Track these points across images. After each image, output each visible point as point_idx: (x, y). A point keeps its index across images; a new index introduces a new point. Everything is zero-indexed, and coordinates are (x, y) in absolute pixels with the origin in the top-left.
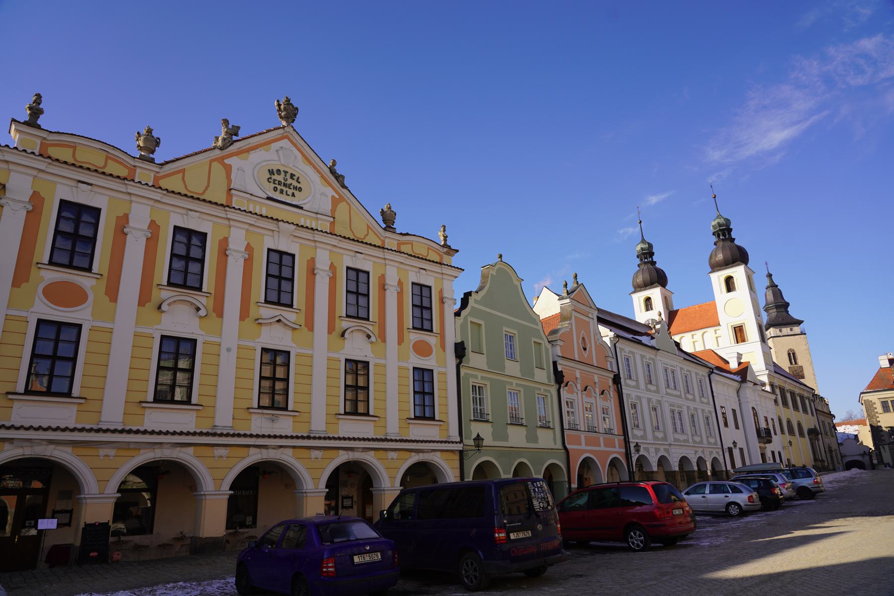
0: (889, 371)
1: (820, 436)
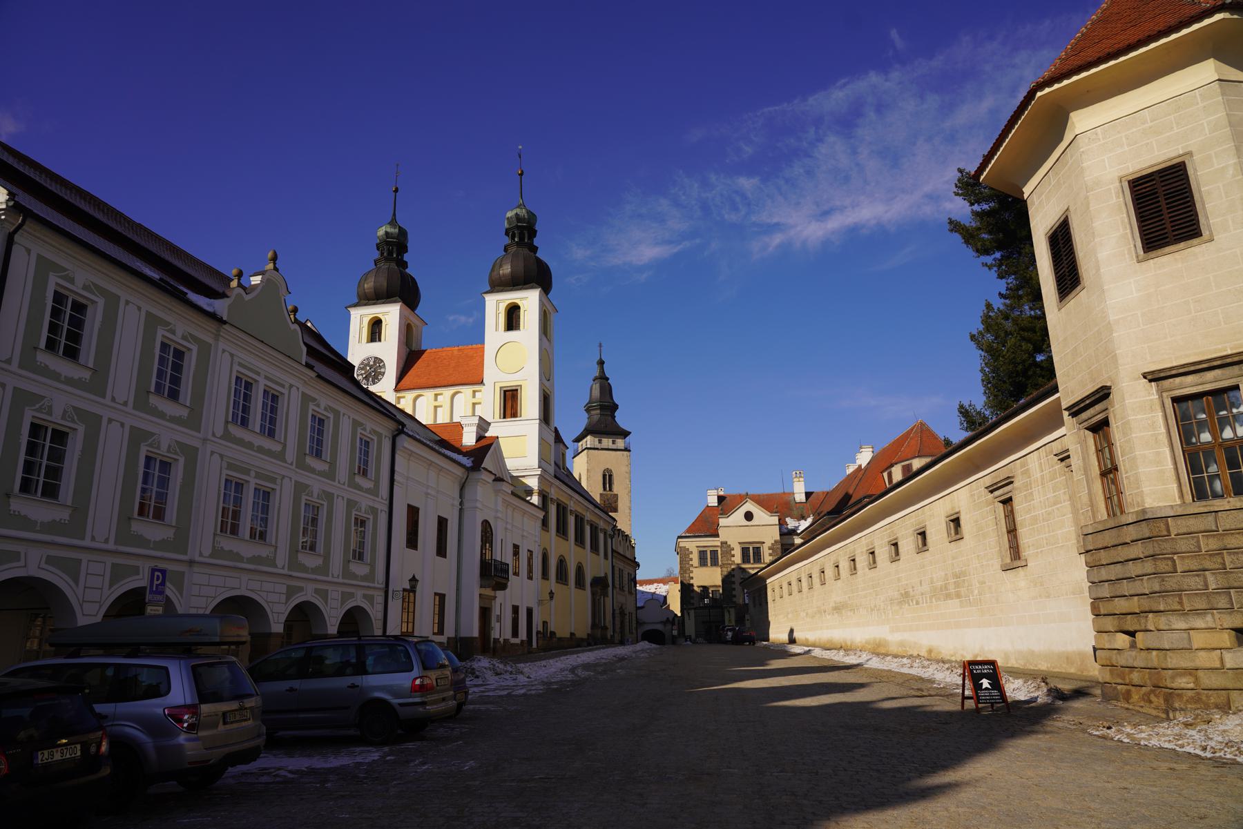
0: (716, 512)
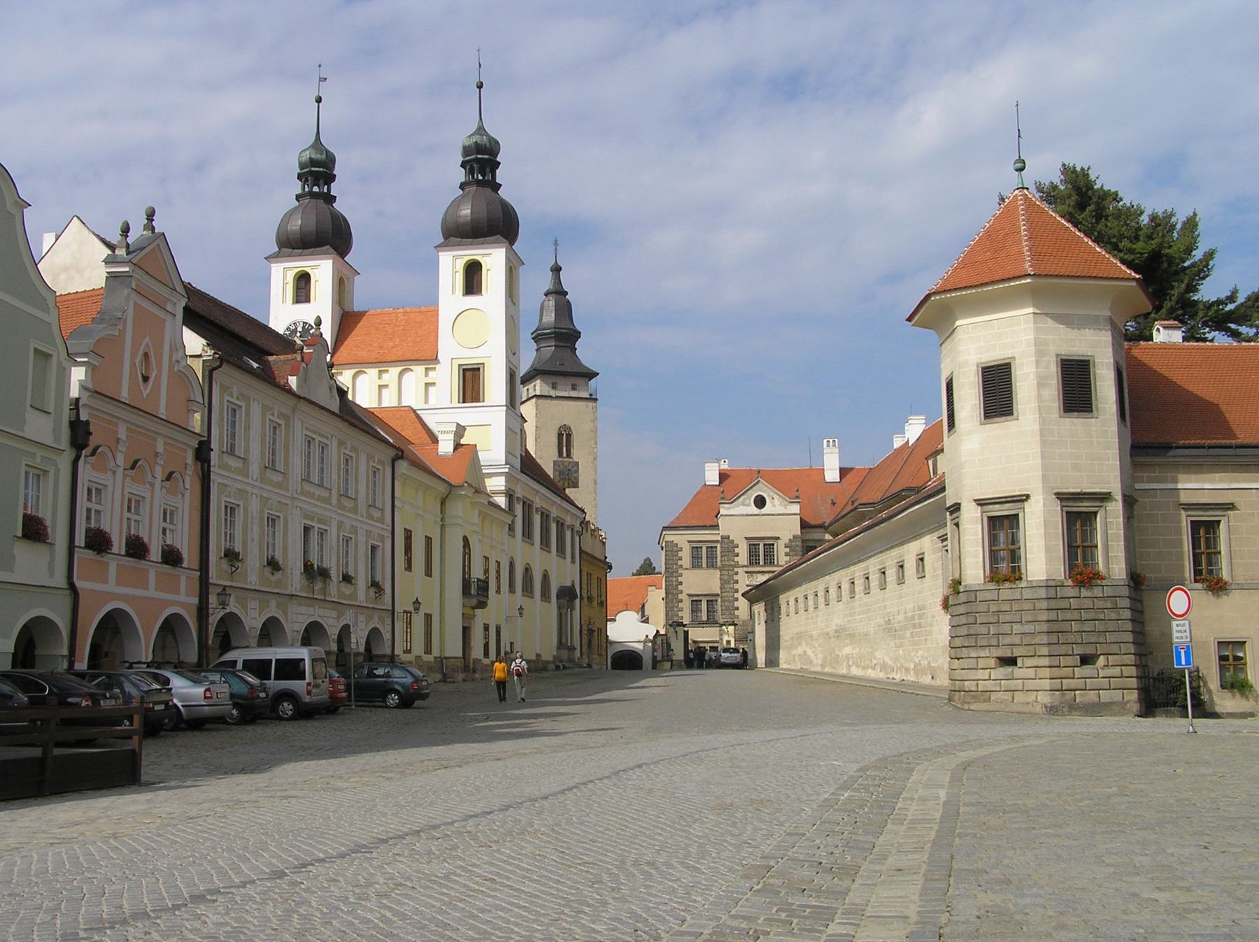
1: (578, 600)
